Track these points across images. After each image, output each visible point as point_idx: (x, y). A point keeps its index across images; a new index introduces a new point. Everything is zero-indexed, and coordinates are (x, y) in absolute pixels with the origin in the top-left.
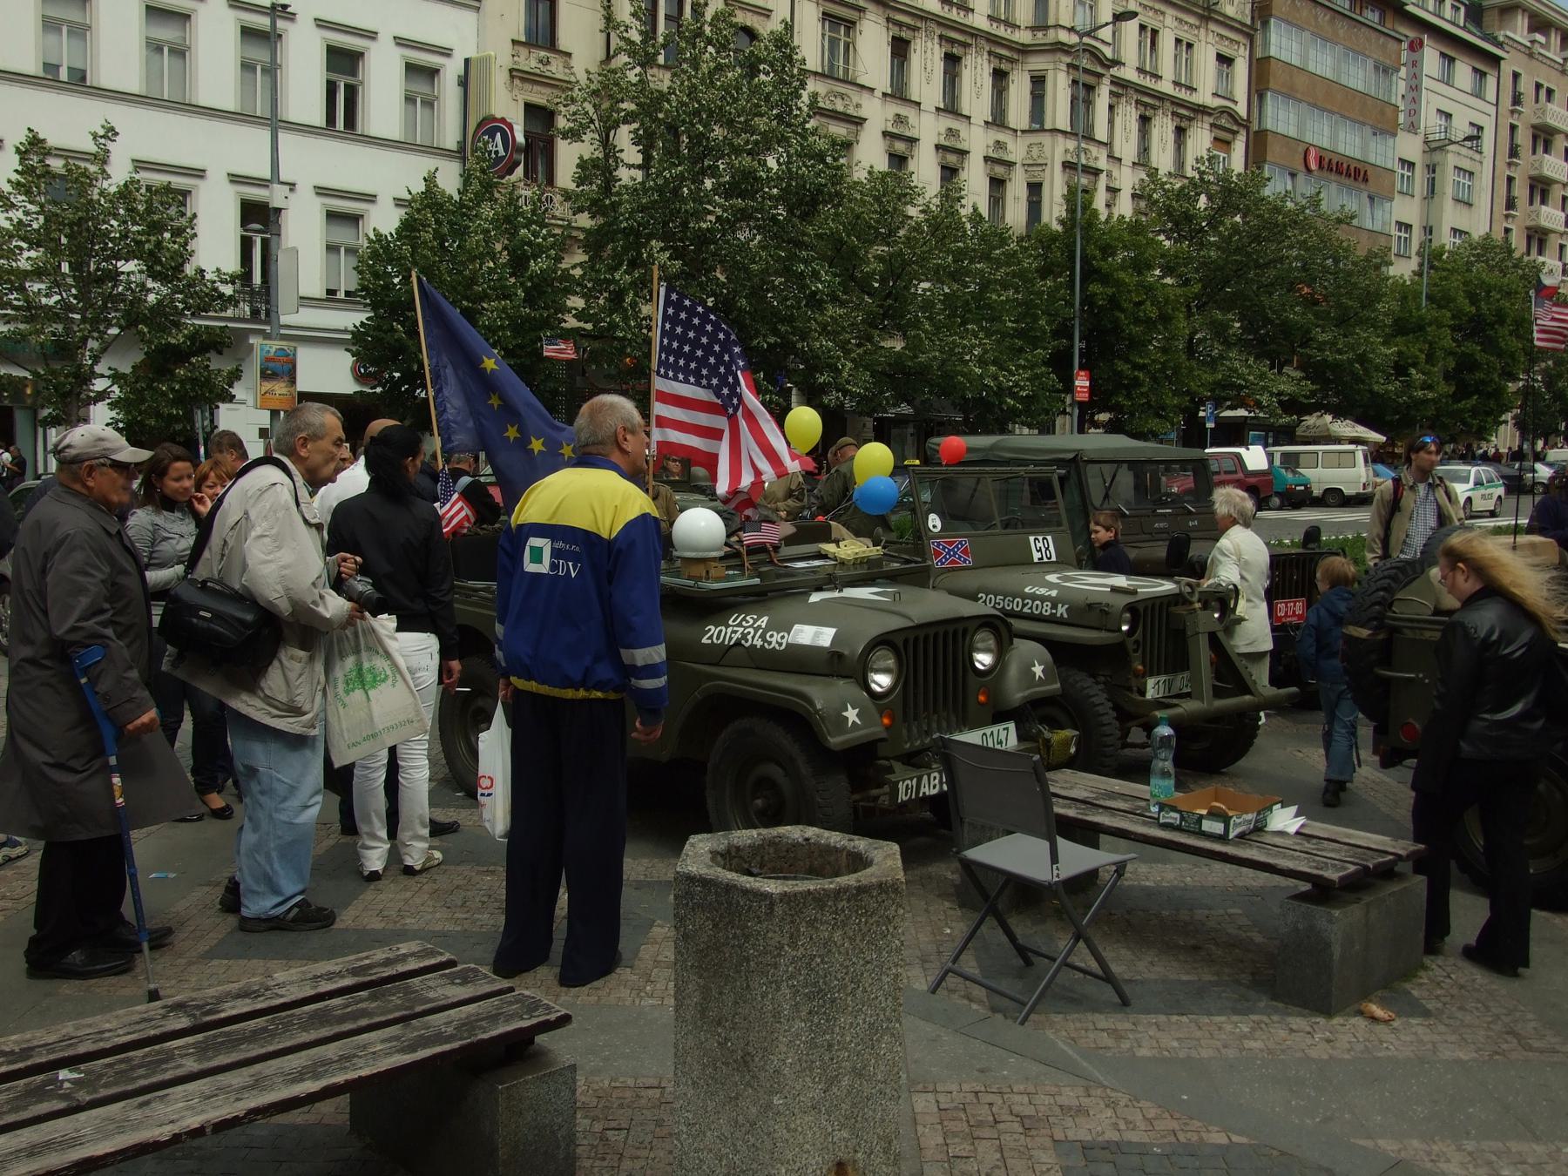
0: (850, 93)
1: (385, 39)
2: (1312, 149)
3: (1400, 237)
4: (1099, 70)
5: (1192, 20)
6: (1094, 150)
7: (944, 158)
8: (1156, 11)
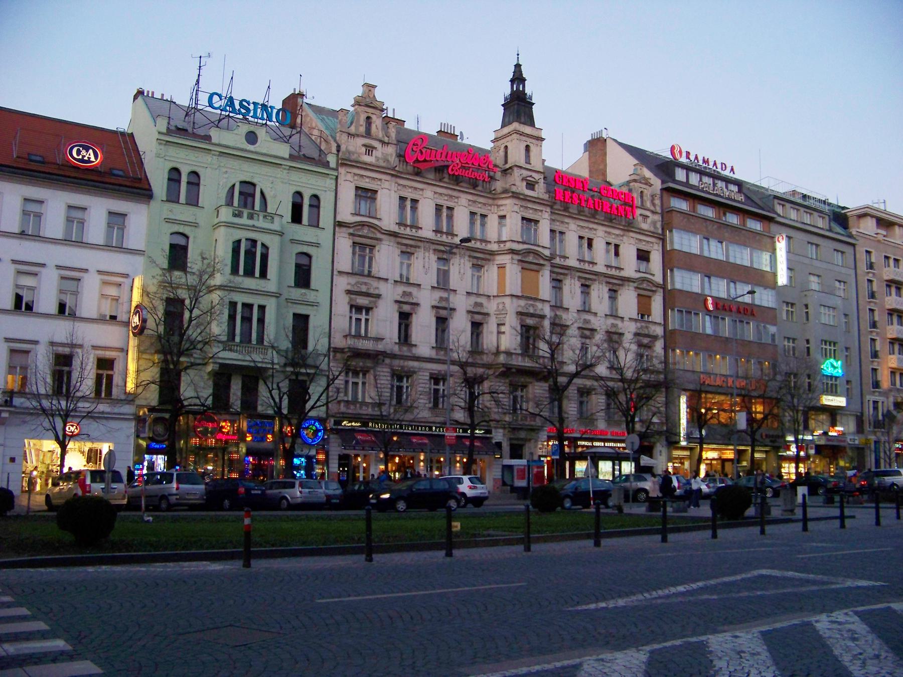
0: (372, 283)
2: (709, 298)
3: (826, 349)
6: (539, 305)
7: (472, 317)
8: (591, 229)
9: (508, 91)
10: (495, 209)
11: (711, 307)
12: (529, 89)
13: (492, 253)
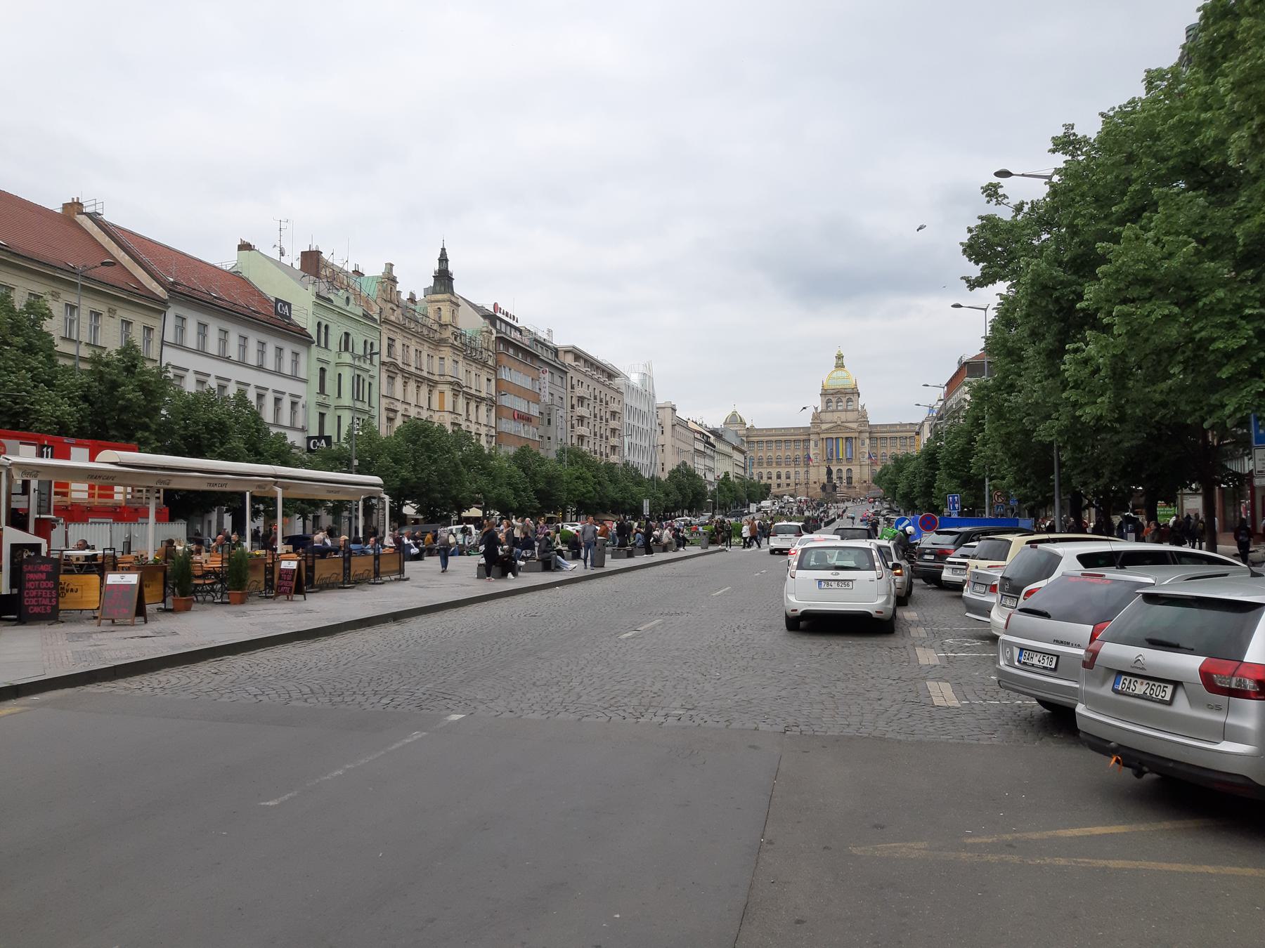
1: (213, 377)
4: (459, 389)
5: (480, 367)
9: (437, 268)
10: (437, 352)
11: (516, 417)
12: (451, 267)
13: (436, 383)
